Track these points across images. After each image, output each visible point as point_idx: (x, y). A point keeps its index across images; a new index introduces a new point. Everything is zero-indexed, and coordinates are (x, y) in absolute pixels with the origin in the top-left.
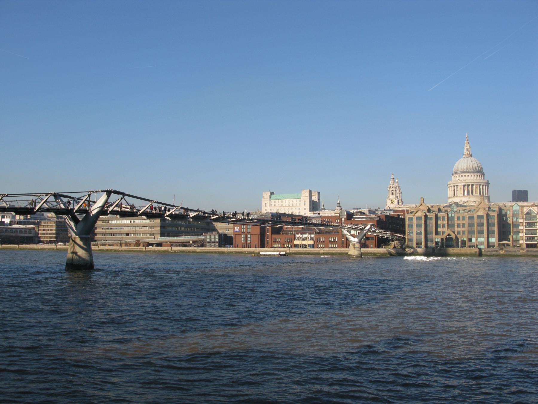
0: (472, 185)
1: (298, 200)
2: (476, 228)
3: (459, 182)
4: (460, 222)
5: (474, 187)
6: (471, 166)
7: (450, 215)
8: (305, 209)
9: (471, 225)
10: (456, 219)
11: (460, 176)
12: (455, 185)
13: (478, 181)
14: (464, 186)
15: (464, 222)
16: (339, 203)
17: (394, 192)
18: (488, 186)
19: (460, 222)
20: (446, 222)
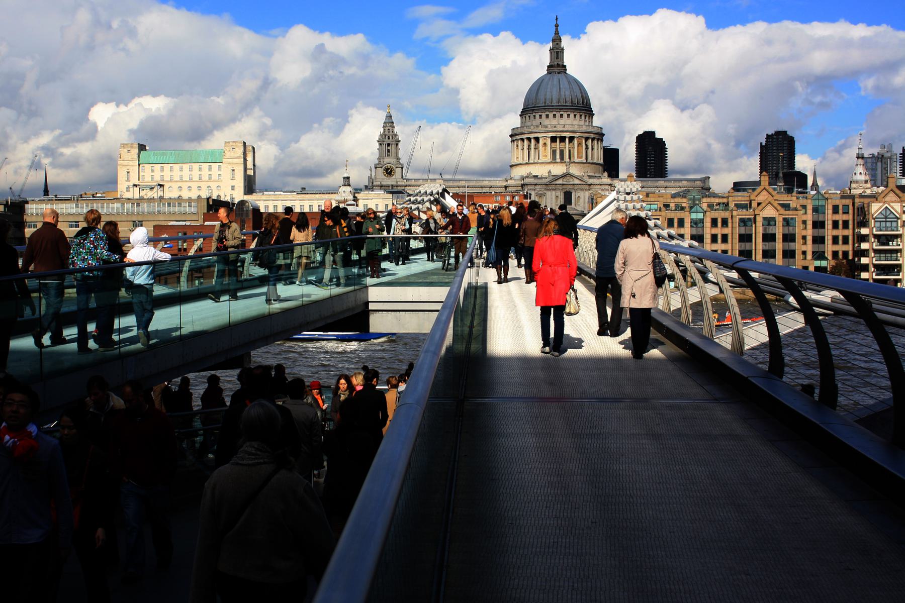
0: (571, 139)
1: (215, 166)
2: (758, 246)
3: (541, 129)
4: (719, 231)
5: (576, 141)
6: (567, 93)
7: (694, 216)
8: (233, 188)
9: (745, 238)
10: (708, 223)
11: (544, 115)
12: (532, 136)
13: (584, 129)
14: (553, 139)
15: (727, 231)
16: (348, 178)
17: (392, 148)
18: (602, 140)
19: (719, 231)
20: (687, 230)
